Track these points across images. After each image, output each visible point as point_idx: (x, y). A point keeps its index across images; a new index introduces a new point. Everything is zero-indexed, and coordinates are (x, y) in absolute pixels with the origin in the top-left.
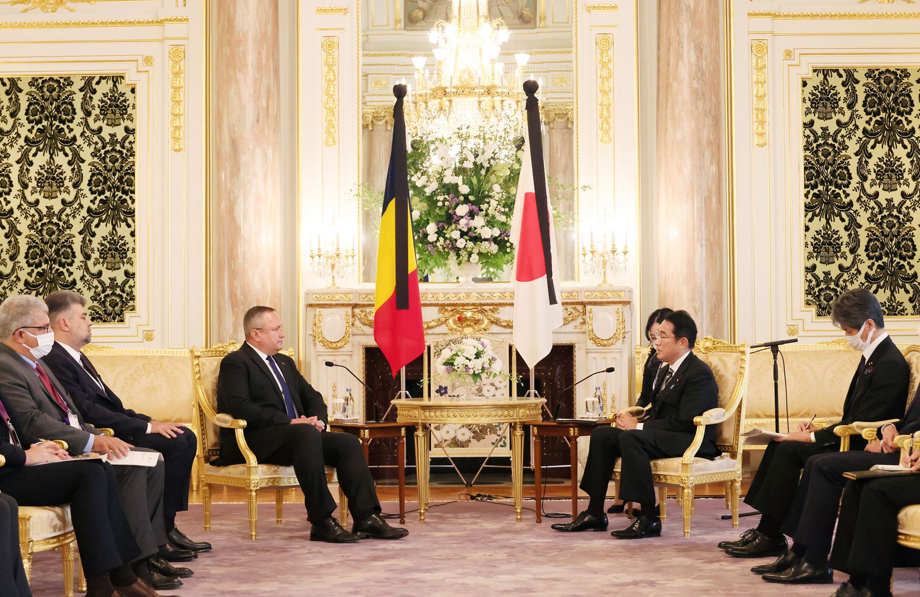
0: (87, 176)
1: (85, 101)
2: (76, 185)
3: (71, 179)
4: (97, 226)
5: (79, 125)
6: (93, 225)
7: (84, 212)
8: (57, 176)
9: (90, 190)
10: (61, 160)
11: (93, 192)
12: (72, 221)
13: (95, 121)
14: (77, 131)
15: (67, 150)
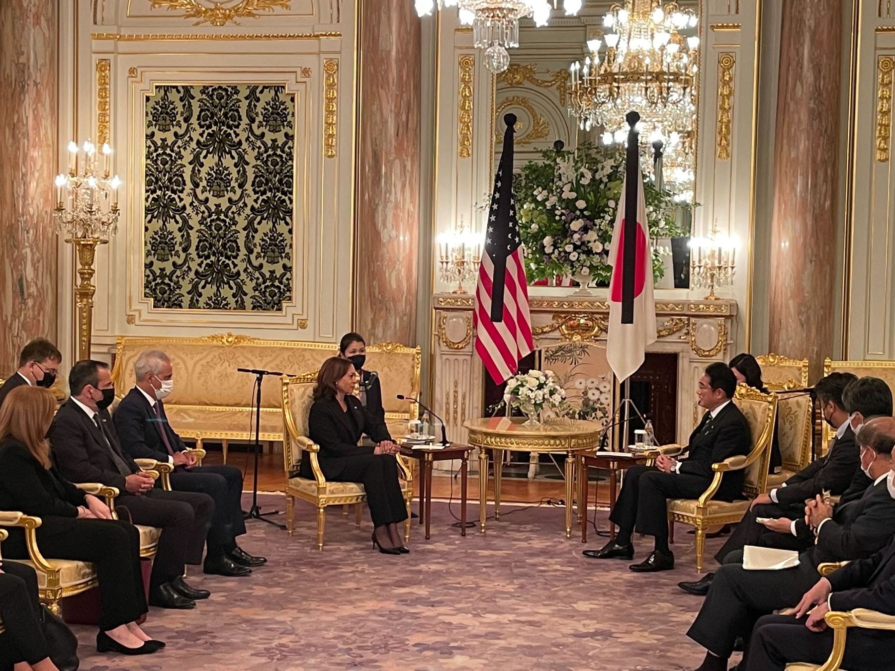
0: (251, 177)
1: (250, 108)
2: (241, 186)
3: (237, 180)
4: (259, 223)
5: (244, 130)
6: (256, 222)
7: (248, 211)
8: (225, 177)
9: (254, 190)
10: (228, 161)
11: (256, 192)
12: (237, 218)
13: (259, 127)
14: (243, 136)
15: (233, 153)
